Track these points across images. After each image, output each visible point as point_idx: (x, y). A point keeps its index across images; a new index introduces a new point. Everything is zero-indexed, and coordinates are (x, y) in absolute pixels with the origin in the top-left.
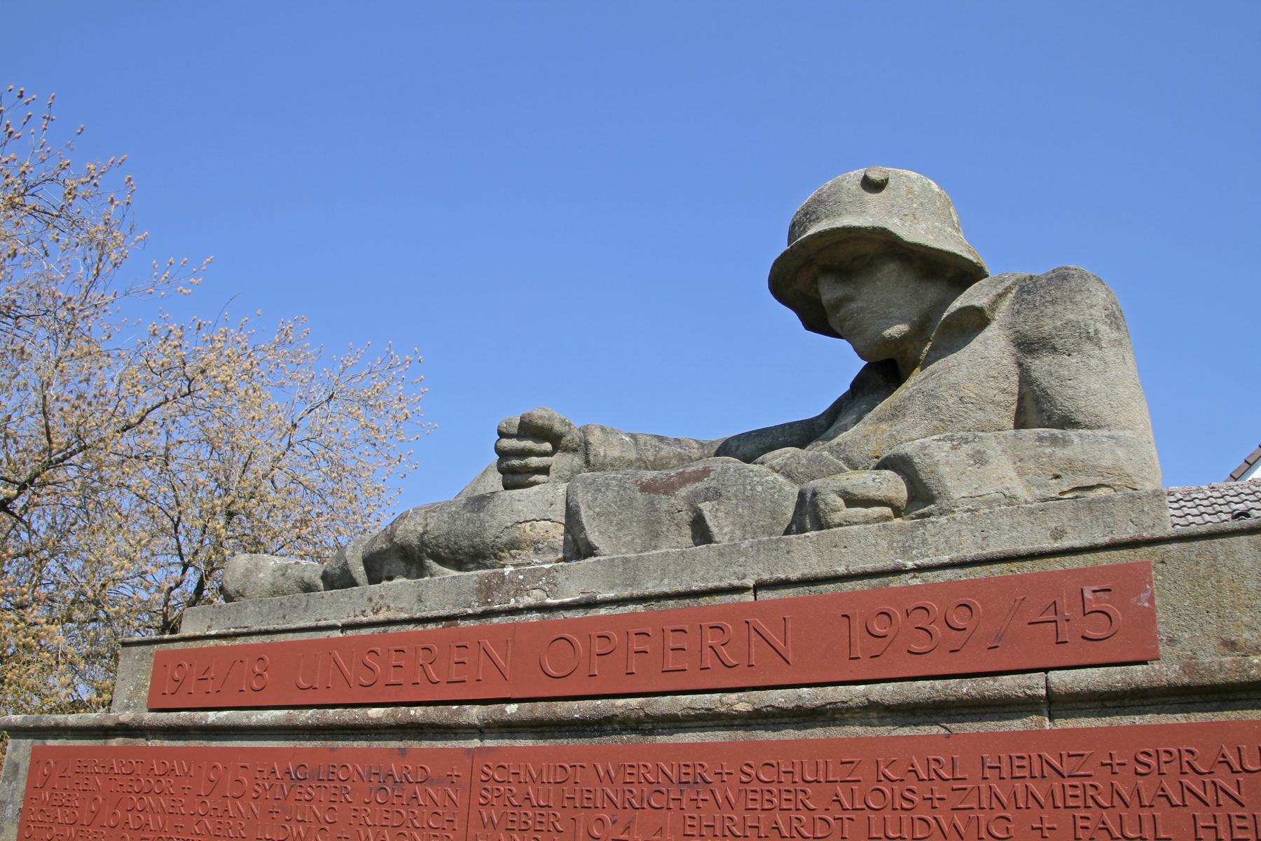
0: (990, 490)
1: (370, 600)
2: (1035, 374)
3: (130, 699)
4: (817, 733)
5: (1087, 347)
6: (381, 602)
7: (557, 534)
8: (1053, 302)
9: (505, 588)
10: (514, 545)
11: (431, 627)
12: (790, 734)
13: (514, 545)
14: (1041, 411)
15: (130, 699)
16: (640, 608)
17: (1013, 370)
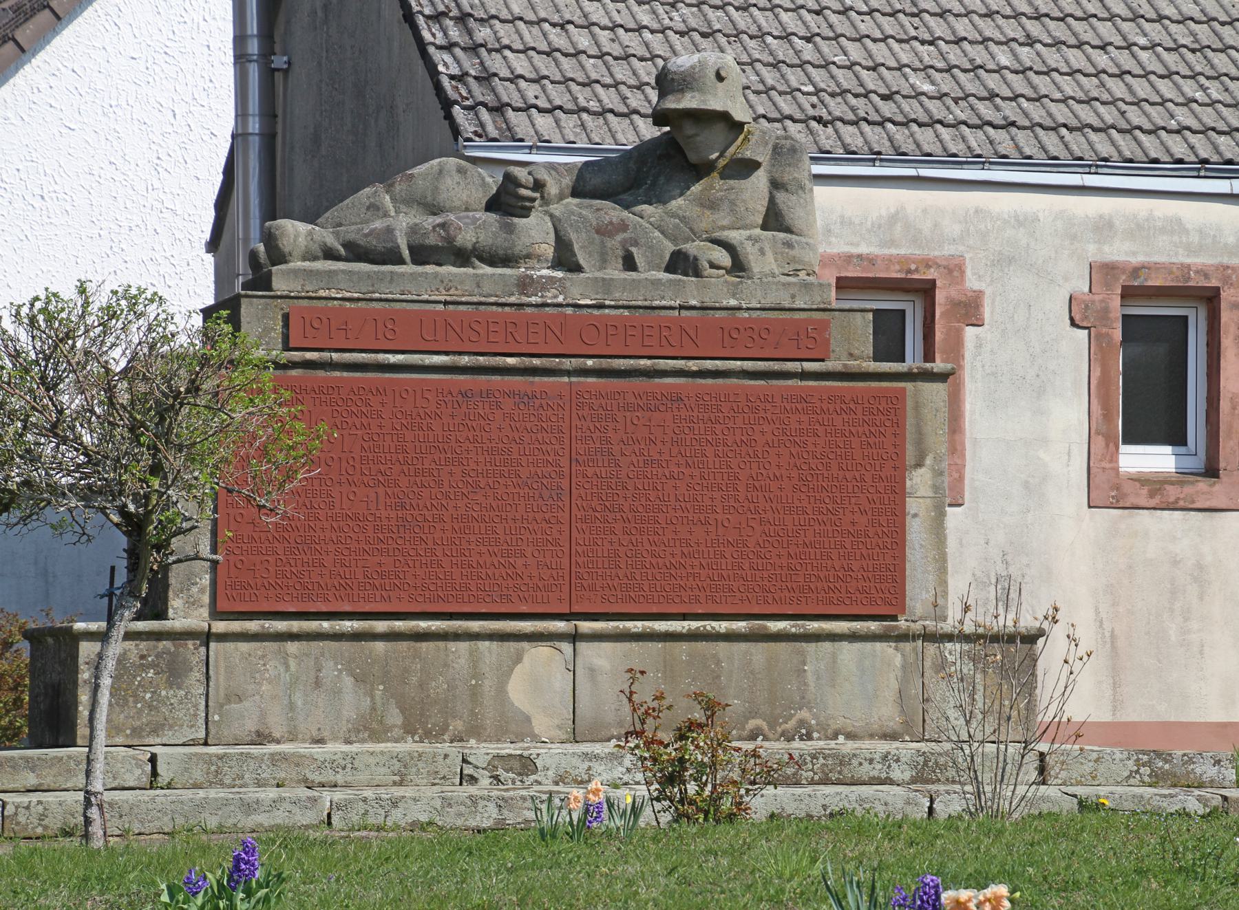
0: (767, 270)
1: (442, 282)
2: (778, 201)
3: (260, 338)
4: (720, 381)
5: (800, 192)
6: (450, 284)
7: (548, 250)
8: (789, 165)
9: (534, 286)
10: (528, 256)
11: (507, 309)
12: (710, 381)
13: (528, 256)
14: (777, 220)
15: (260, 338)
16: (626, 313)
17: (767, 196)
